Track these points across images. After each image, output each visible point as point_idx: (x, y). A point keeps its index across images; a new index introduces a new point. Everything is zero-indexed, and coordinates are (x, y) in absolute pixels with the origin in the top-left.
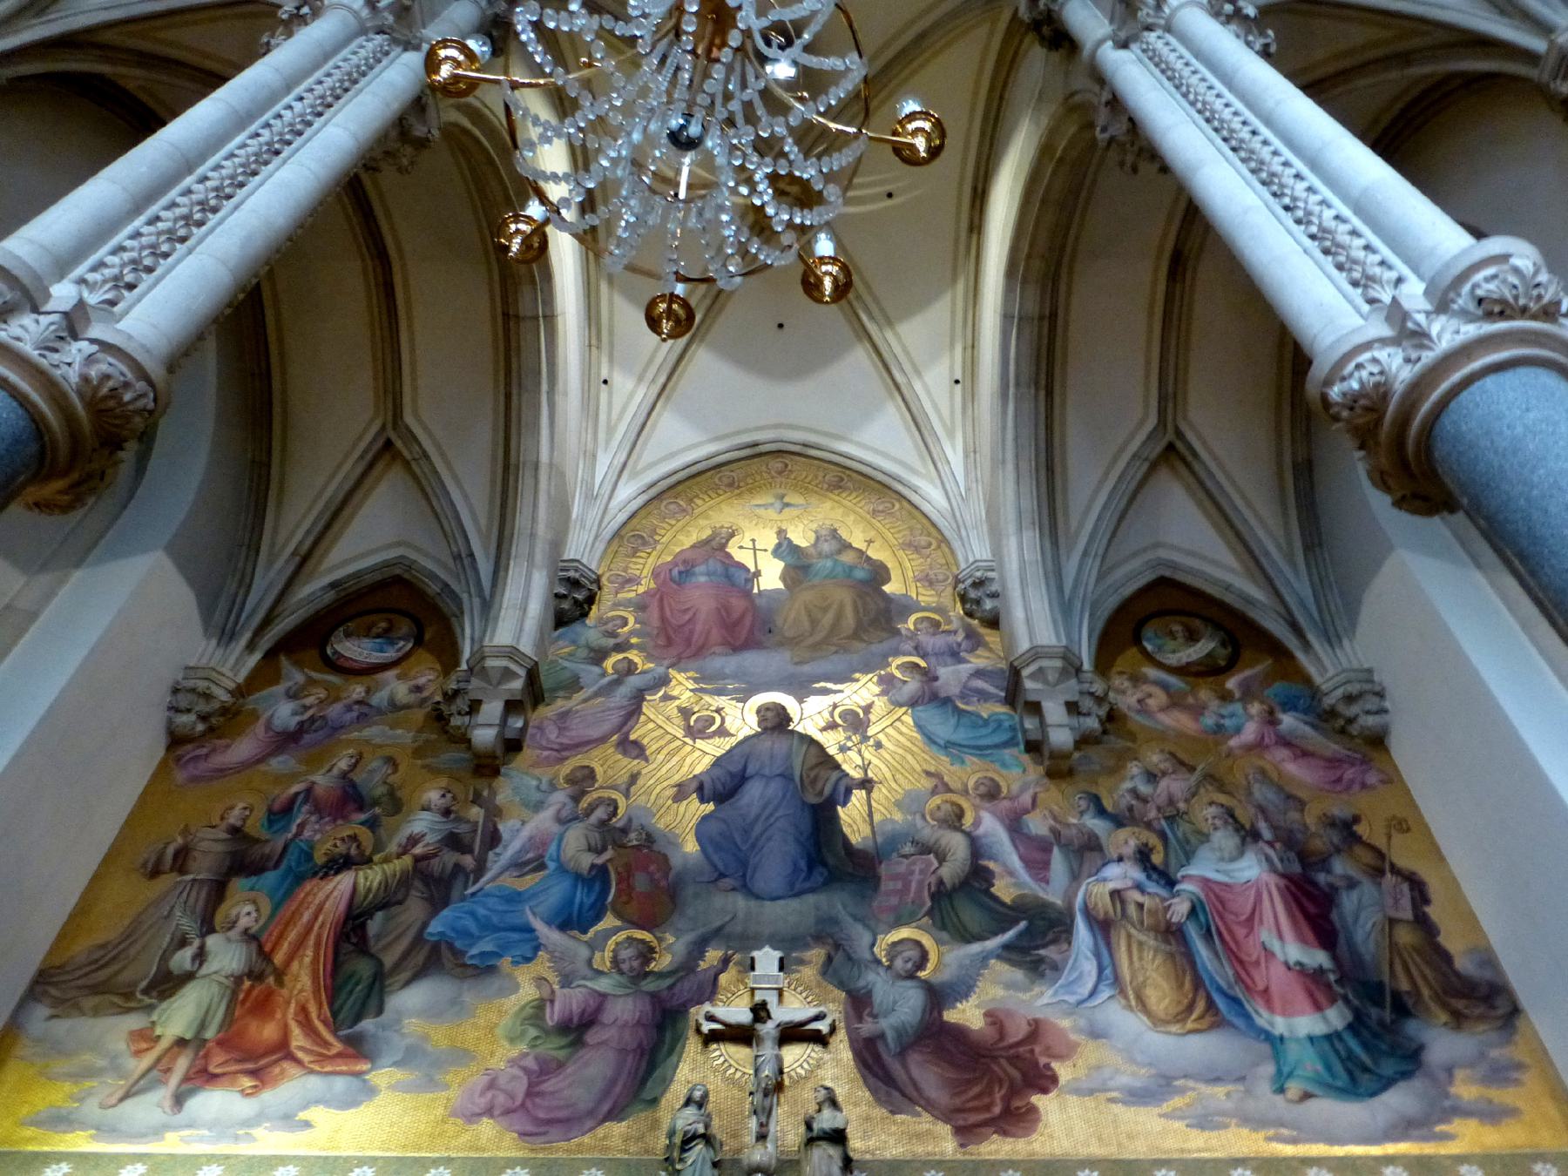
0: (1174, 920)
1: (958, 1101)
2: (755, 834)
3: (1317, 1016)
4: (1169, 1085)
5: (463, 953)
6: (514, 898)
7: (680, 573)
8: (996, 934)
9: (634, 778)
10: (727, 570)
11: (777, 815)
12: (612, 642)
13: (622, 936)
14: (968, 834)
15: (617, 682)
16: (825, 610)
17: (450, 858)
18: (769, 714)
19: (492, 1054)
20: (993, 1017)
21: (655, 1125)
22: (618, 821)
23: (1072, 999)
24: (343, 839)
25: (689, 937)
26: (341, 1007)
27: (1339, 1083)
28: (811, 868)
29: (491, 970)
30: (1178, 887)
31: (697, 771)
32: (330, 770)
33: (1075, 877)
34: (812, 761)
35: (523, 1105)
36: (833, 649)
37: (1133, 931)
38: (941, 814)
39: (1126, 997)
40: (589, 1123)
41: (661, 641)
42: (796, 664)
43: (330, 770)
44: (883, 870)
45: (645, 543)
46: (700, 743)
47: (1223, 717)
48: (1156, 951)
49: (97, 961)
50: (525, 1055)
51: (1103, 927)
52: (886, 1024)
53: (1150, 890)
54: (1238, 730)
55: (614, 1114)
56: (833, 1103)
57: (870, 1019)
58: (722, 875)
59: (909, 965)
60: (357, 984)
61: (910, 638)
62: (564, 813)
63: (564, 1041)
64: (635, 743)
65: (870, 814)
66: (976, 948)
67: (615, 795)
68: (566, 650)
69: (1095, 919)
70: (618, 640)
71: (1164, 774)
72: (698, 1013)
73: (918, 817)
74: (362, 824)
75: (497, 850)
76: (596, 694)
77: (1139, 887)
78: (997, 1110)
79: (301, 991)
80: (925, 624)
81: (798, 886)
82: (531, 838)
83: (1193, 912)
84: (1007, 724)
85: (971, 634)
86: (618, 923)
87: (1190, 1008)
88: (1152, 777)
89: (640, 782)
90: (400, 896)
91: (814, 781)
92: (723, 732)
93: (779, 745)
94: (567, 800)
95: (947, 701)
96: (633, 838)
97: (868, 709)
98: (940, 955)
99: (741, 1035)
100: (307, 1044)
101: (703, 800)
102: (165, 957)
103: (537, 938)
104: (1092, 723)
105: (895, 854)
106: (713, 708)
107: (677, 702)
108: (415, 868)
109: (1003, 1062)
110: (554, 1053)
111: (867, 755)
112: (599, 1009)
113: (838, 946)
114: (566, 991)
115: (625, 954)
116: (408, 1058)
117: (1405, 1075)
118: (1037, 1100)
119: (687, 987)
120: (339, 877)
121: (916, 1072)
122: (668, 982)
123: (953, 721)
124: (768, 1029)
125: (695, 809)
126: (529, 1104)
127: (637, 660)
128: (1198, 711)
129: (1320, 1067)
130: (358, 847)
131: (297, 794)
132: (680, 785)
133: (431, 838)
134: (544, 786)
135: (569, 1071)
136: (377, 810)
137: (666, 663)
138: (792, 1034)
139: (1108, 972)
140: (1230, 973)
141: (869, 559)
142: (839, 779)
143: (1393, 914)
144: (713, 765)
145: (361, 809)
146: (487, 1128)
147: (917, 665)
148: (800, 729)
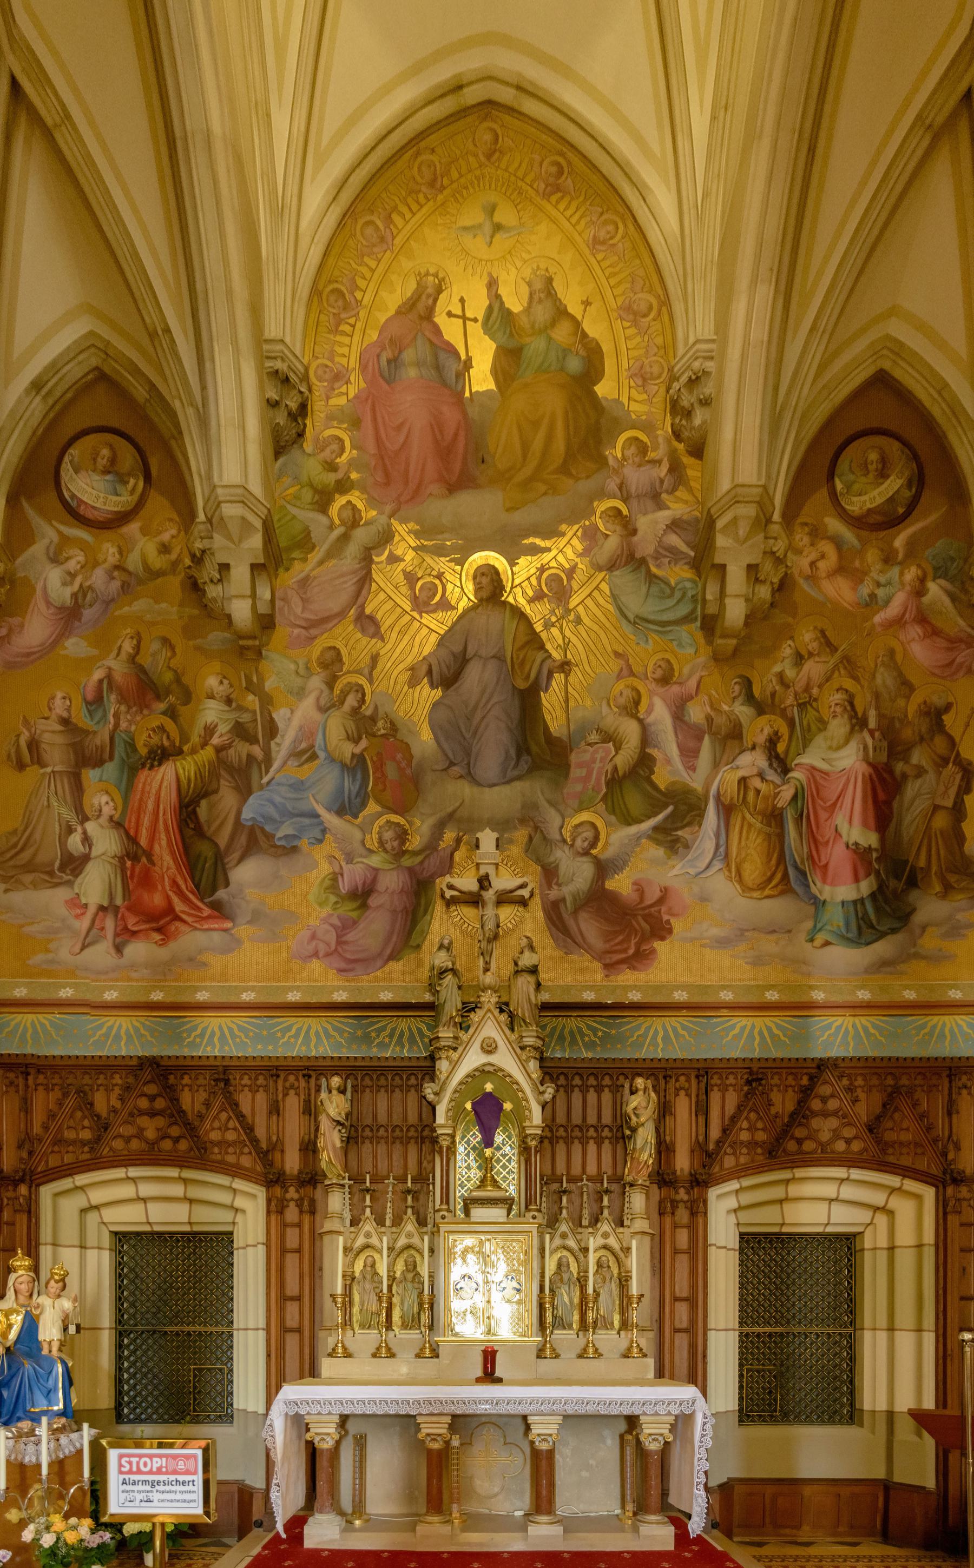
0: (779, 805)
1: (607, 946)
2: (475, 722)
3: (854, 886)
4: (742, 935)
5: (273, 836)
6: (298, 787)
7: (389, 362)
8: (649, 818)
9: (375, 659)
10: (436, 357)
11: (492, 702)
12: (331, 478)
13: (382, 821)
14: (640, 721)
15: (345, 538)
16: (536, 424)
17: (241, 750)
18: (485, 581)
19: (310, 914)
20: (639, 888)
21: (420, 964)
22: (367, 711)
23: (692, 871)
24: (153, 730)
25: (431, 821)
26: (200, 880)
27: (850, 935)
28: (519, 756)
29: (294, 850)
30: (791, 775)
31: (425, 653)
32: (118, 655)
33: (716, 765)
34: (522, 639)
35: (336, 950)
36: (542, 488)
37: (748, 816)
38: (622, 701)
39: (730, 871)
40: (379, 963)
41: (380, 477)
42: (507, 510)
43: (118, 655)
44: (574, 758)
45: (346, 307)
46: (426, 619)
47: (879, 585)
48: (759, 832)
49: (15, 845)
50: (331, 915)
51: (727, 810)
52: (567, 891)
53: (768, 778)
54: (887, 602)
55: (394, 956)
56: (531, 948)
57: (555, 887)
58: (452, 764)
59: (586, 844)
60: (205, 862)
61: (616, 472)
62: (322, 702)
63: (355, 905)
64: (371, 618)
65: (567, 701)
66: (634, 829)
67: (363, 681)
68: (291, 491)
69: (723, 804)
70: (340, 475)
71: (811, 654)
72: (442, 883)
73: (604, 703)
74: (164, 713)
75: (277, 740)
76: (329, 555)
77: (761, 775)
78: (631, 952)
79: (168, 868)
80: (633, 449)
81: (510, 774)
82: (301, 728)
83: (795, 797)
84: (690, 594)
85: (676, 468)
86: (379, 809)
87: (770, 880)
88: (799, 659)
89: (380, 665)
90: (214, 785)
91: (522, 663)
92: (445, 605)
93: (492, 620)
94: (324, 687)
95: (643, 562)
96: (381, 727)
97: (571, 572)
98: (608, 835)
99: (474, 900)
100: (186, 909)
101: (433, 686)
102: (63, 844)
103: (322, 823)
104: (764, 592)
105: (583, 743)
106: (434, 573)
107: (402, 565)
108: (218, 757)
109: (640, 918)
110: (351, 914)
111: (568, 633)
112: (374, 880)
113: (536, 828)
114: (351, 866)
115: (388, 835)
116: (256, 917)
117: (894, 931)
118: (658, 945)
119: (433, 863)
120: (163, 768)
121: (583, 926)
122: (420, 858)
123: (644, 589)
124: (489, 895)
125: (428, 695)
126: (340, 949)
127: (360, 505)
128: (858, 577)
129: (842, 924)
130: (168, 737)
131: (101, 681)
132: (412, 669)
133: (223, 728)
134: (302, 671)
135: (361, 926)
136: (172, 698)
137: (388, 509)
138: (504, 899)
139: (722, 850)
140: (806, 850)
141: (584, 335)
142: (543, 661)
143: (939, 802)
144: (438, 645)
145: (158, 698)
146: (316, 966)
147: (619, 512)
148: (511, 600)
